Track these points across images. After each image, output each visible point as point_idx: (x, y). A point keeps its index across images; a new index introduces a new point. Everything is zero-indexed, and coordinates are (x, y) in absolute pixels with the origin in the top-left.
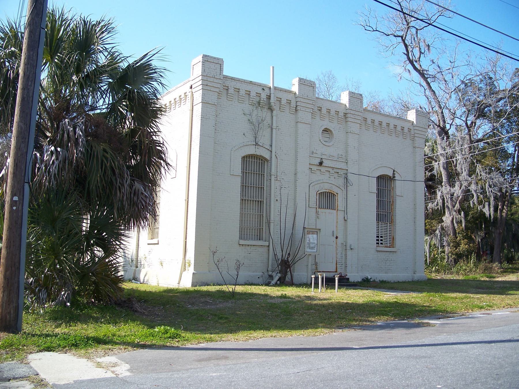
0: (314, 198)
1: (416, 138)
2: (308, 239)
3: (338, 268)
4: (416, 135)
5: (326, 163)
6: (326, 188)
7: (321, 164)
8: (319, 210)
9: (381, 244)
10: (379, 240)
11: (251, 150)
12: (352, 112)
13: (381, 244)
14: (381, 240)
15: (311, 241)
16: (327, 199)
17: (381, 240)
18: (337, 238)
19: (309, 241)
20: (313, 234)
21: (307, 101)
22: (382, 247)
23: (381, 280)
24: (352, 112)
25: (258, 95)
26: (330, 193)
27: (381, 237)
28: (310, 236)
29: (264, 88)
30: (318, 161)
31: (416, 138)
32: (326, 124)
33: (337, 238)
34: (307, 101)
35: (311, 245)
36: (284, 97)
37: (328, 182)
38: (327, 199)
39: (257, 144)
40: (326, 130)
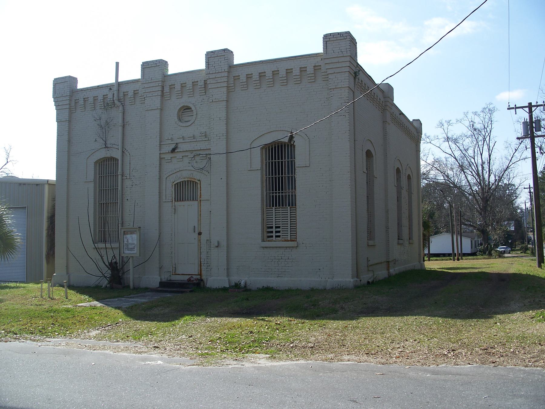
0: (169, 192)
1: (330, 76)
2: (125, 240)
3: (203, 270)
4: (329, 71)
5: (182, 147)
6: (184, 176)
7: (173, 150)
8: (176, 203)
9: (279, 236)
10: (270, 232)
11: (103, 154)
12: (211, 76)
13: (276, 236)
14: (276, 232)
15: (130, 241)
16: (186, 190)
17: (276, 232)
18: (200, 234)
19: (128, 241)
20: (131, 234)
21: (152, 85)
22: (279, 241)
23: (265, 286)
24: (211, 76)
25: (105, 97)
26: (190, 181)
27: (276, 227)
28: (128, 236)
29: (111, 87)
30: (173, 146)
31: (330, 76)
32: (185, 101)
33: (200, 234)
34: (152, 85)
35: (130, 246)
36: (130, 90)
37: (181, 169)
38: (186, 190)
39: (106, 147)
40: (186, 109)
